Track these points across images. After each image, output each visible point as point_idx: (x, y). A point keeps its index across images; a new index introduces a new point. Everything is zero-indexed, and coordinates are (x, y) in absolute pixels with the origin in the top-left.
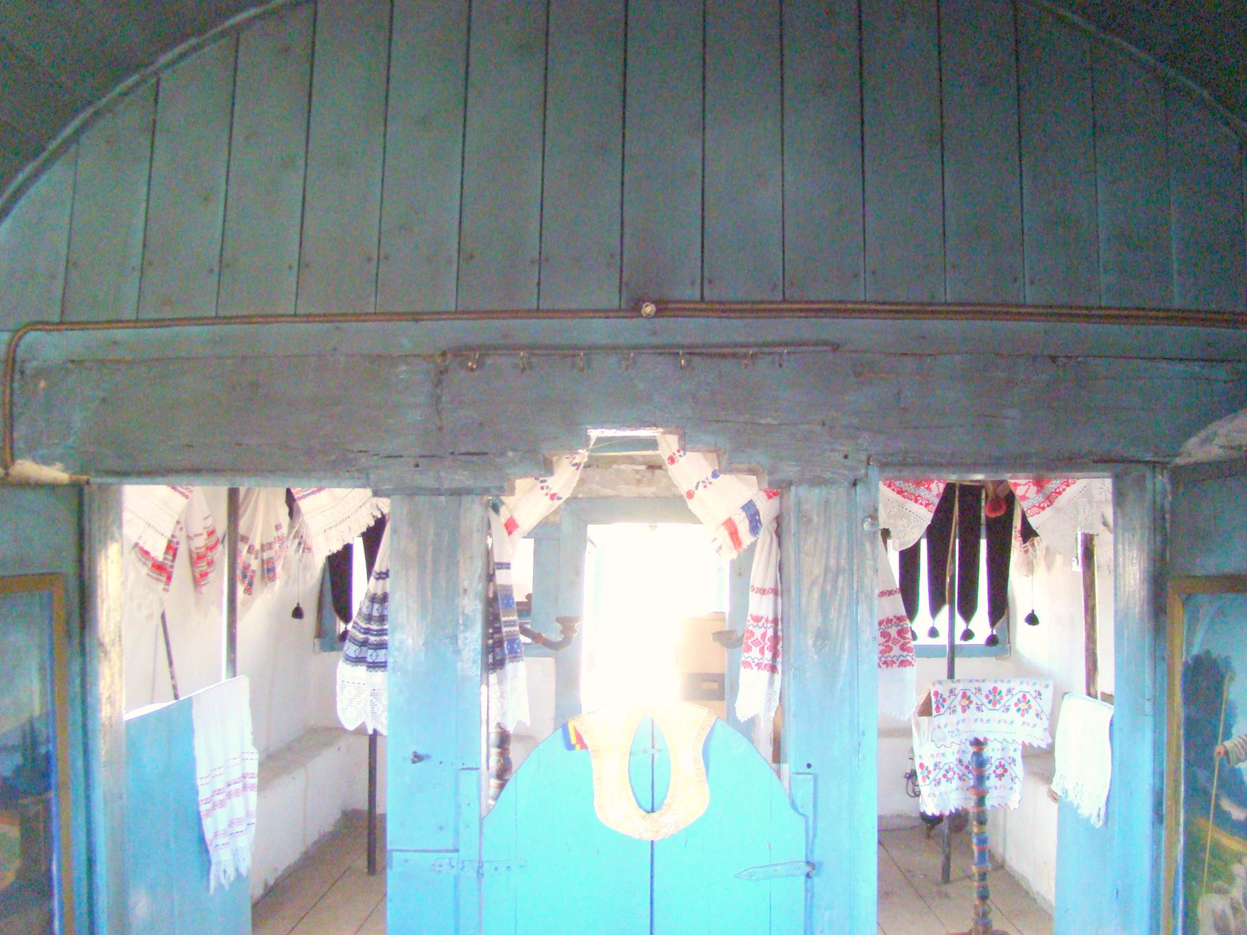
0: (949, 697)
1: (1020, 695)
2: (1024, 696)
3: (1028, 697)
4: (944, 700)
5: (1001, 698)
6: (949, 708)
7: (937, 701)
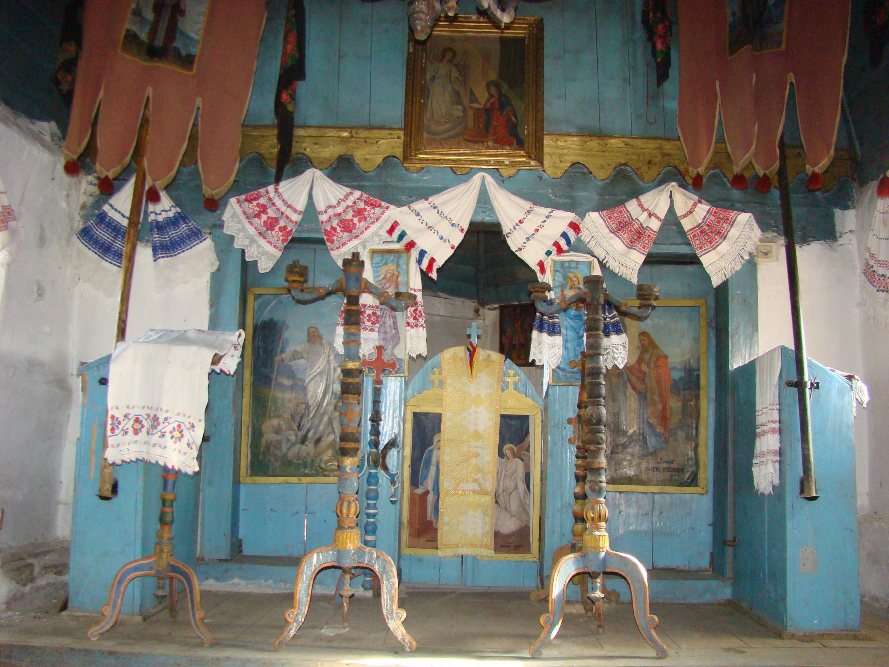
0: (124, 420)
1: (176, 425)
2: (179, 426)
3: (183, 427)
4: (119, 423)
5: (158, 424)
6: (123, 430)
7: (112, 424)
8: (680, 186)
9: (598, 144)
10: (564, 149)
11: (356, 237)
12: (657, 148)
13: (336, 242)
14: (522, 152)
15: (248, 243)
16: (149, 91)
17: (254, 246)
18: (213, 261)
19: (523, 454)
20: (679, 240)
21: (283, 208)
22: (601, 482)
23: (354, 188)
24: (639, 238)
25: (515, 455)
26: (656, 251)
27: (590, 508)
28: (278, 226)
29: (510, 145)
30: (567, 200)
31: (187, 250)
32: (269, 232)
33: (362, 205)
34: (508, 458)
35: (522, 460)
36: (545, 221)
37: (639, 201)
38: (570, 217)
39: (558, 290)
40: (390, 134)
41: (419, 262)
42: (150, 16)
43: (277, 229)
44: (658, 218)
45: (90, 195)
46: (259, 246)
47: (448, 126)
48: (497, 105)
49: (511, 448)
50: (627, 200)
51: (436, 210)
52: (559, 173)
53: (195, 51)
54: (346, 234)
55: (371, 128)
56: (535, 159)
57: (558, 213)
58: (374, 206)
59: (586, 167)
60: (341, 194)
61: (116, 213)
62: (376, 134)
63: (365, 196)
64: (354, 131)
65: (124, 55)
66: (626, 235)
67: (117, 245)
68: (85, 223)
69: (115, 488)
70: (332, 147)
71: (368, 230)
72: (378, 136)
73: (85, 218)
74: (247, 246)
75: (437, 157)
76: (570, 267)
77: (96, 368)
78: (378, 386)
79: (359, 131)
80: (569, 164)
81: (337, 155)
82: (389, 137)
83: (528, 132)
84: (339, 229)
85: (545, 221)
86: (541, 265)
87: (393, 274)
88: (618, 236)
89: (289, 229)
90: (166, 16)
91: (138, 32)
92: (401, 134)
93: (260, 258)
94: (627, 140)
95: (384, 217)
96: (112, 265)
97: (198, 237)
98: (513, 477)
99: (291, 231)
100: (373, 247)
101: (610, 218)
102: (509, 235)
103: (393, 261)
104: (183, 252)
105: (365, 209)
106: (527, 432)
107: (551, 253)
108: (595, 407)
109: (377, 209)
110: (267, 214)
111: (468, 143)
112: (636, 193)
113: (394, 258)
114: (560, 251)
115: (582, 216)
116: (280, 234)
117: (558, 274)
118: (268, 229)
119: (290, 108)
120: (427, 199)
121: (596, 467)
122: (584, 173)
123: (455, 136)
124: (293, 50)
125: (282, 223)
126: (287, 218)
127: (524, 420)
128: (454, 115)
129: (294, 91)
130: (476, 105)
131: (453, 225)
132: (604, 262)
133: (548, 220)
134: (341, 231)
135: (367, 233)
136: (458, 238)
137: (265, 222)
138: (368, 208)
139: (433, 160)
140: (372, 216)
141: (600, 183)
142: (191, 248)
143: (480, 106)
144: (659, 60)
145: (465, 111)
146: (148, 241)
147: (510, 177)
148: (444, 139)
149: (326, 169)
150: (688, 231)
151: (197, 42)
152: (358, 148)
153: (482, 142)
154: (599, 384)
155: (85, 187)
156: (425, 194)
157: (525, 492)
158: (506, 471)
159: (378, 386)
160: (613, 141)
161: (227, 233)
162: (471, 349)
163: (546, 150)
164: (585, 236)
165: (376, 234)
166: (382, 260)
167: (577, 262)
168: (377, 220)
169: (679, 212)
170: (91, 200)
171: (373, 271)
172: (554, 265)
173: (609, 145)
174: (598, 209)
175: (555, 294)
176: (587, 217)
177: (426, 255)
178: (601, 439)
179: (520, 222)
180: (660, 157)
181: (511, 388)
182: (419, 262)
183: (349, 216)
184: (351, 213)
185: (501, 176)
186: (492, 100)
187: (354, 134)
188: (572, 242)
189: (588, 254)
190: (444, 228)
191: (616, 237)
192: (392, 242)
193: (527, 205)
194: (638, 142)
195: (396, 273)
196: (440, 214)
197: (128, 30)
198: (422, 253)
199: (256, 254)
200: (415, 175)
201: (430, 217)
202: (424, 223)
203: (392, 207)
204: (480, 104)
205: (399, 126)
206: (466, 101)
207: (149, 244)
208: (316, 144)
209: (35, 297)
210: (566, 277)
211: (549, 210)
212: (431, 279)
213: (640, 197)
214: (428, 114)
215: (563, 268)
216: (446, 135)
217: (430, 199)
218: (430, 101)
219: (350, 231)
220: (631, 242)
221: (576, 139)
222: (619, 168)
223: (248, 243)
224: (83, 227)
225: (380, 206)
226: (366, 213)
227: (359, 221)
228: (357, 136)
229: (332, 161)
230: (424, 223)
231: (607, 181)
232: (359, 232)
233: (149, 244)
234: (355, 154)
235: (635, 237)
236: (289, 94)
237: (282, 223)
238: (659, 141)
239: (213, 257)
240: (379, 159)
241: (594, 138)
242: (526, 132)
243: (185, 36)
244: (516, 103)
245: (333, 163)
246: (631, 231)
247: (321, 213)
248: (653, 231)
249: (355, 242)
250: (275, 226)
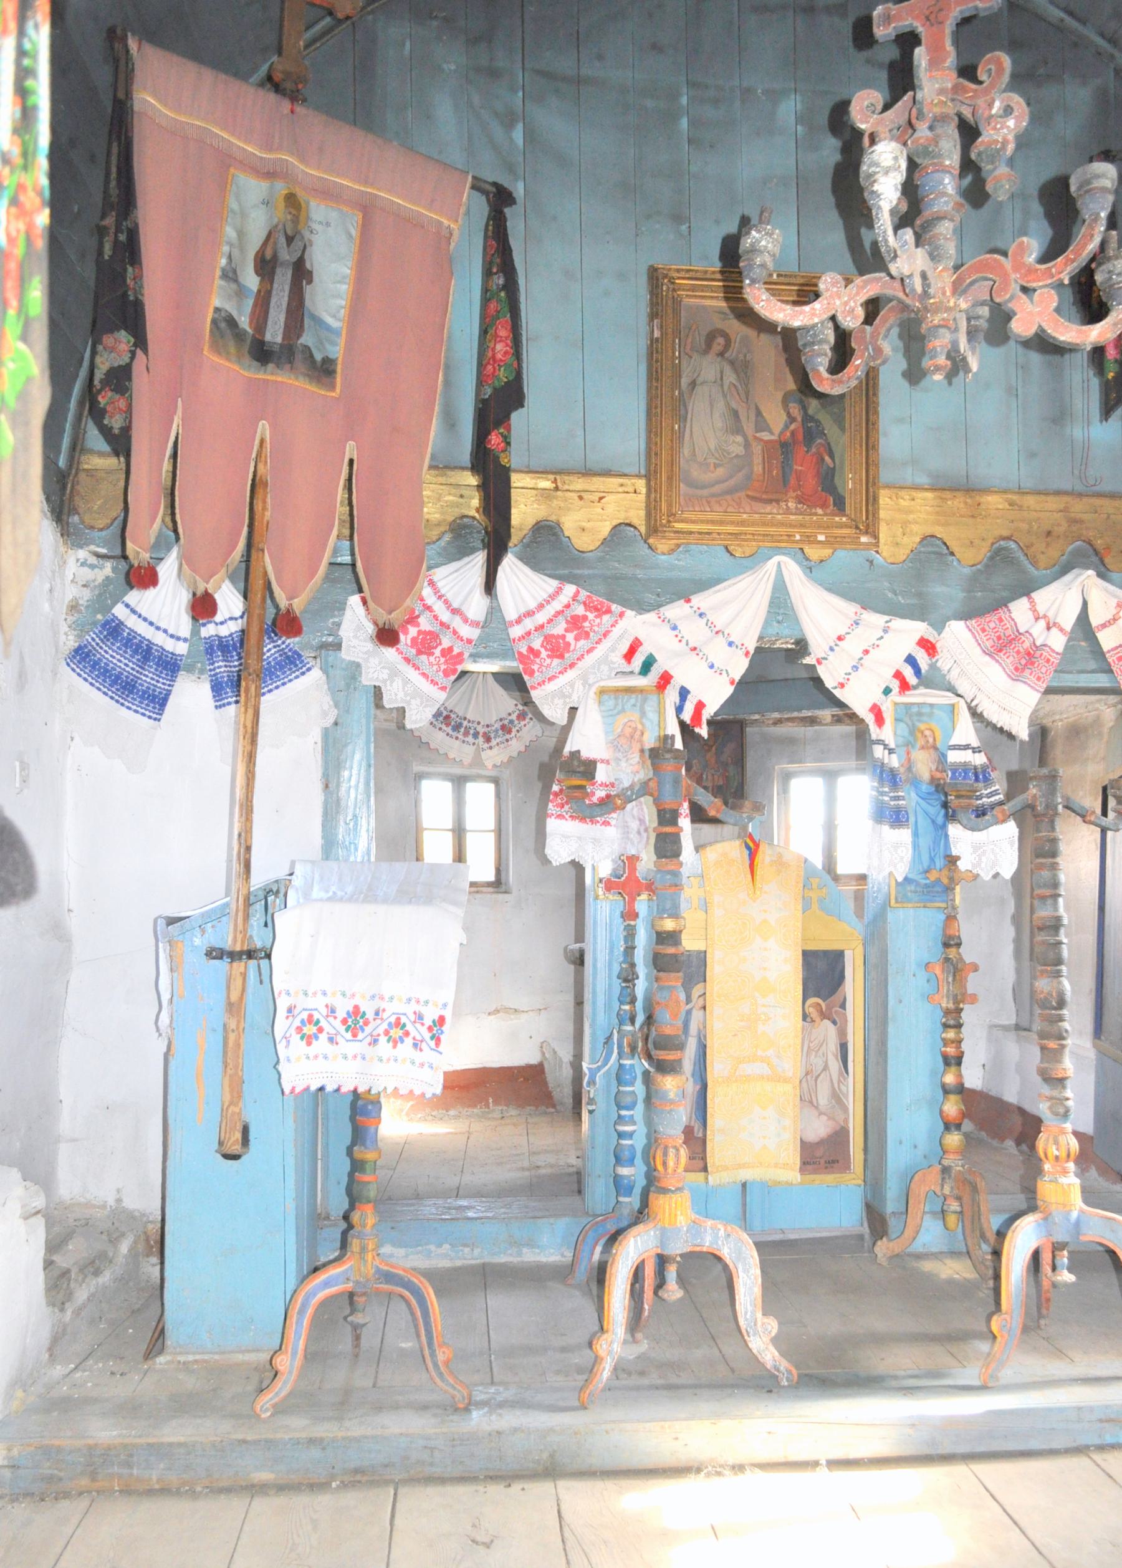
8: (1100, 575)
9: (966, 503)
10: (911, 512)
11: (572, 665)
12: (1061, 511)
13: (537, 674)
14: (844, 519)
15: (386, 677)
16: (264, 428)
17: (398, 683)
18: (326, 707)
19: (834, 1014)
20: (1093, 665)
21: (445, 616)
22: (1068, 1099)
23: (564, 579)
24: (1033, 663)
25: (824, 1016)
26: (1055, 684)
27: (1051, 1141)
28: (439, 648)
29: (824, 506)
30: (914, 601)
31: (277, 687)
32: (424, 657)
33: (580, 610)
34: (813, 1021)
35: (834, 1023)
36: (882, 638)
37: (1032, 603)
38: (919, 628)
39: (902, 751)
40: (622, 485)
41: (679, 709)
42: (252, 281)
43: (437, 652)
44: (1062, 630)
45: (84, 586)
46: (406, 681)
47: (720, 472)
48: (800, 437)
49: (819, 1004)
50: (1013, 599)
51: (705, 620)
52: (902, 554)
53: (336, 351)
54: (556, 661)
55: (588, 473)
56: (866, 533)
57: (898, 623)
58: (601, 611)
59: (945, 544)
60: (545, 590)
61: (140, 620)
62: (598, 483)
63: (584, 594)
65: (216, 359)
66: (1008, 661)
67: (148, 680)
68: (79, 636)
69: (245, 1140)
70: (522, 506)
71: (591, 655)
72: (602, 488)
73: (80, 628)
74: (384, 681)
75: (704, 527)
76: (920, 714)
77: (198, 932)
78: (632, 923)
79: (571, 478)
80: (918, 540)
82: (621, 490)
83: (854, 483)
84: (544, 654)
85: (882, 638)
86: (877, 712)
87: (635, 729)
88: (997, 661)
89: (456, 651)
90: (283, 280)
91: (235, 314)
92: (641, 484)
93: (409, 703)
94: (1015, 497)
95: (616, 632)
96: (138, 716)
97: (296, 666)
98: (821, 1052)
99: (460, 654)
100: (603, 684)
101: (984, 630)
102: (824, 661)
103: (634, 705)
104: (270, 691)
105: (585, 618)
106: (842, 977)
107: (891, 691)
108: (1055, 981)
109: (606, 618)
110: (418, 625)
111: (753, 503)
112: (1026, 589)
113: (637, 700)
114: (905, 686)
115: (939, 627)
116: (443, 660)
117: (902, 725)
118: (419, 653)
119: (504, 461)
120: (688, 601)
121: (1060, 1076)
122: (940, 554)
123: (730, 492)
124: (506, 353)
125: (446, 641)
126: (455, 632)
127: (835, 959)
128: (729, 454)
129: (509, 429)
130: (765, 436)
131: (730, 644)
132: (973, 704)
133: (886, 636)
134: (548, 656)
135: (589, 659)
136: (739, 667)
137: (414, 640)
138: (591, 616)
139: (700, 533)
140: (596, 629)
141: (967, 571)
142: (284, 684)
143: (773, 438)
144: (1111, 375)
145: (747, 445)
146: (202, 671)
147: (822, 561)
148: (713, 495)
150: (1109, 652)
151: (337, 333)
152: (569, 509)
153: (777, 501)
154: (1060, 943)
155: (73, 570)
156: (684, 590)
157: (841, 1074)
158: (810, 1042)
159: (632, 923)
160: (990, 498)
161: (348, 658)
162: (751, 845)
163: (882, 514)
164: (944, 662)
165: (605, 660)
166: (616, 705)
167: (932, 705)
168: (605, 635)
169: (1095, 620)
170: (86, 595)
171: (604, 723)
172: (896, 710)
173: (983, 507)
174: (965, 616)
175: (899, 758)
176: (947, 629)
177: (689, 697)
178: (1066, 1031)
179: (840, 638)
180: (1065, 524)
181: (815, 906)
182: (679, 709)
183: (559, 628)
184: (564, 625)
185: (807, 559)
186: (793, 427)
187: (559, 484)
188: (923, 671)
189: (948, 690)
190: (718, 651)
191: (993, 662)
192: (632, 672)
193: (850, 609)
194: (1030, 501)
195: (640, 727)
196: (710, 624)
198: (684, 693)
199: (401, 695)
200: (663, 557)
201: (694, 631)
202: (684, 641)
203: (629, 613)
204: (772, 433)
205: (634, 470)
206: (749, 427)
207: (205, 677)
209: (17, 785)
210: (913, 731)
211: (887, 618)
212: (699, 736)
213: (1033, 595)
214: (686, 451)
215: (910, 715)
216: (717, 489)
217: (696, 600)
218: (688, 425)
219: (562, 657)
220: (1017, 669)
221: (929, 495)
222: (997, 545)
223: (386, 677)
224: (77, 645)
225: (609, 611)
226: (586, 624)
227: (577, 639)
228: (566, 487)
229: (525, 532)
230: (684, 641)
231: (979, 567)
232: (576, 657)
233: (205, 677)
234: (563, 519)
235: (1023, 662)
236: (501, 434)
237: (446, 641)
238: (1066, 499)
239: (327, 701)
240: (605, 529)
241: (958, 494)
242: (849, 482)
243: (318, 321)
244: (830, 429)
246: (1018, 652)
247: (511, 624)
248: (1053, 651)
249: (571, 674)
250: (436, 648)
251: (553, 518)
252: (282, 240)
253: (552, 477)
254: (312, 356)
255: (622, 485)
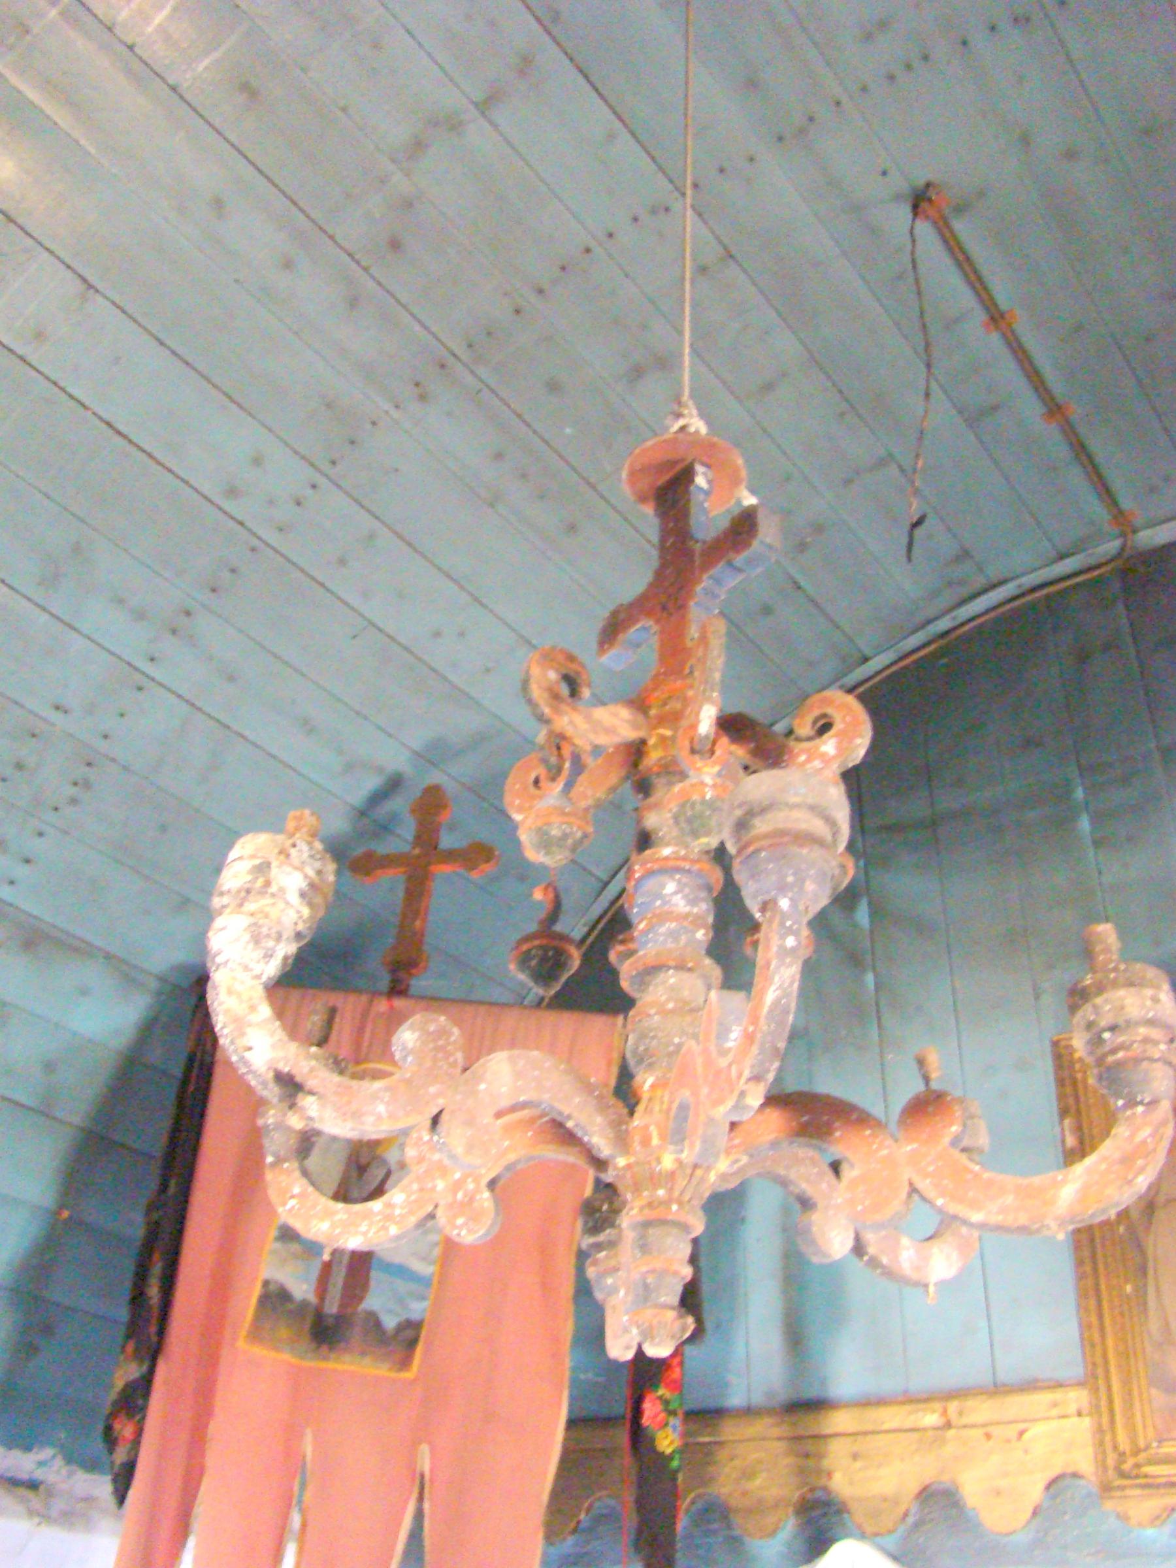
40: (1055, 1405)
55: (998, 1389)
64: (953, 1406)
79: (970, 1403)
81: (914, 1487)
82: (1054, 1412)
149: (890, 1532)
197: (266, 1283)
208: (855, 1456)
228: (965, 1420)
229: (902, 1508)
245: (906, 1515)
251: (945, 1478)
252: (354, 1174)
253: (937, 1406)
254: (378, 1324)
255: (1055, 1405)
